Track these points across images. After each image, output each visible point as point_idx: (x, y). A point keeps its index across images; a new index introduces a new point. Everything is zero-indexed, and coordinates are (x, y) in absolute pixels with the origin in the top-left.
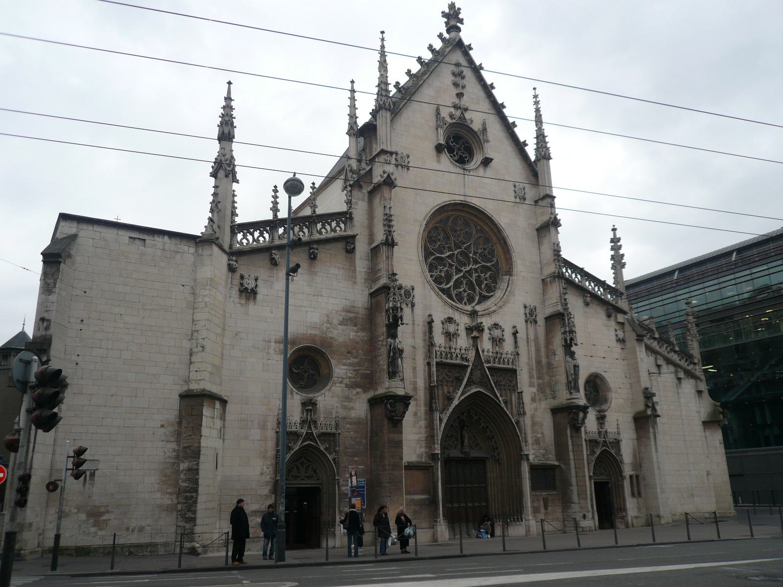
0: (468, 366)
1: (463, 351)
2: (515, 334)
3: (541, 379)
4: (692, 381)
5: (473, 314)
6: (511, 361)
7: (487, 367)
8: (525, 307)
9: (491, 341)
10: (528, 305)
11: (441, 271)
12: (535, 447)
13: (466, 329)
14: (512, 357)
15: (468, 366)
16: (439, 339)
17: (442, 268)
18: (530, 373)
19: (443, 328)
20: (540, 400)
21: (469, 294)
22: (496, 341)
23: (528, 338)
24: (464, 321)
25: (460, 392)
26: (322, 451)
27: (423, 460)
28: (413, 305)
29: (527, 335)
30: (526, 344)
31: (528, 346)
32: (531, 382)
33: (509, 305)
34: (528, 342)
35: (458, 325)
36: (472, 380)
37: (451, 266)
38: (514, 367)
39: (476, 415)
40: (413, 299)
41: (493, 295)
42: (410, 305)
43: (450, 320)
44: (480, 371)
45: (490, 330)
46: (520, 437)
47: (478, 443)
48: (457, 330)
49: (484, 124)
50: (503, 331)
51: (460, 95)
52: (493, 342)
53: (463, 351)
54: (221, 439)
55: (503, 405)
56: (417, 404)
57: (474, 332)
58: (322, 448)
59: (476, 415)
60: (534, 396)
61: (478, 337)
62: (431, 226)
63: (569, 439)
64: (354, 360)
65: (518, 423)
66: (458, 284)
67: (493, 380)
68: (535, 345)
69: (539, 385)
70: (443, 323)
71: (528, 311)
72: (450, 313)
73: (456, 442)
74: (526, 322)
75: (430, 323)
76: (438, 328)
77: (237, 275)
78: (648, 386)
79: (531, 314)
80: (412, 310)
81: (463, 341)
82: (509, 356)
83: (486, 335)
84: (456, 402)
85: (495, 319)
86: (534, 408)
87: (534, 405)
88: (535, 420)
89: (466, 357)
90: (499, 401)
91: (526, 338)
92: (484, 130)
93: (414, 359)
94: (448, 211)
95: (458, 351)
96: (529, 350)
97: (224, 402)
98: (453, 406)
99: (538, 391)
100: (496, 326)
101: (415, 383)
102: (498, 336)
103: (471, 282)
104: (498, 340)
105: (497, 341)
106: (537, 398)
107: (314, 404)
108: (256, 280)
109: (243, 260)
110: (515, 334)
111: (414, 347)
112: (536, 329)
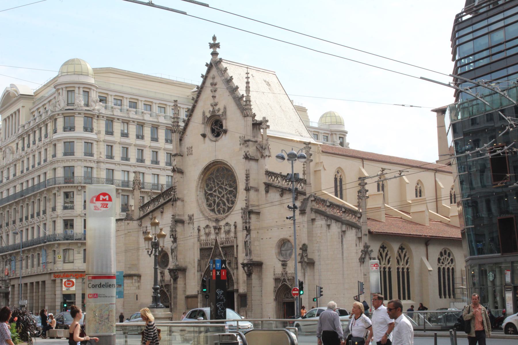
2: (236, 227)
4: (354, 231)
5: (217, 221)
7: (222, 247)
16: (203, 238)
24: (212, 224)
26: (165, 292)
28: (193, 224)
37: (215, 196)
43: (207, 226)
49: (225, 108)
51: (214, 97)
54: (139, 289)
57: (218, 229)
58: (165, 291)
61: (218, 233)
62: (205, 178)
72: (207, 223)
75: (199, 230)
76: (202, 232)
77: (142, 227)
78: (306, 242)
80: (193, 225)
81: (213, 237)
83: (222, 230)
85: (227, 220)
92: (225, 112)
94: (211, 168)
95: (202, 242)
97: (139, 276)
100: (227, 224)
101: (194, 260)
105: (228, 232)
107: (164, 274)
108: (147, 227)
109: (143, 220)
110: (236, 227)
111: (194, 243)
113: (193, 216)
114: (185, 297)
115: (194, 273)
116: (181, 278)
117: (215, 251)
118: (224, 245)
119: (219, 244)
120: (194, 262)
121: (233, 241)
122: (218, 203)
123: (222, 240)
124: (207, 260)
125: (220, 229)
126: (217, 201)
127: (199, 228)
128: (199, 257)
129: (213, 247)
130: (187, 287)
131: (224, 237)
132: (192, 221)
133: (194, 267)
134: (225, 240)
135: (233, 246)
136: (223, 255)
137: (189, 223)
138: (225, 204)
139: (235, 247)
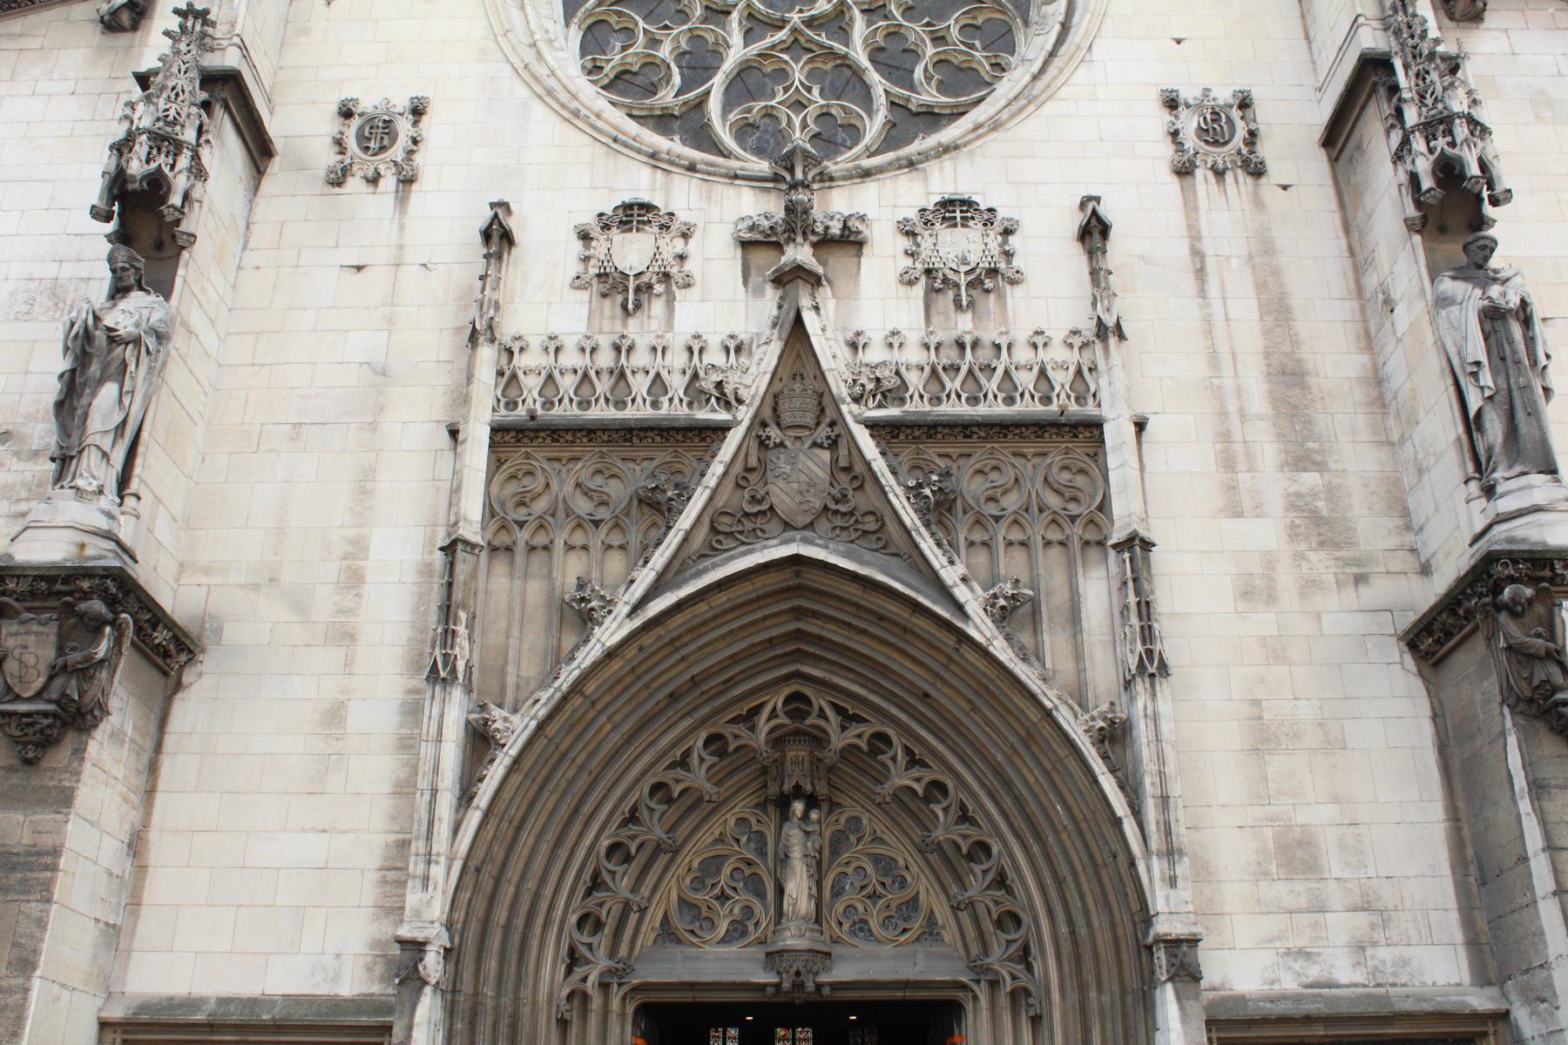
0: (722, 430)
1: (715, 357)
3: (1321, 467)
6: (1061, 379)
7: (873, 426)
8: (1172, 104)
9: (919, 290)
10: (1188, 94)
11: (799, 105)
12: (1281, 891)
13: (745, 245)
14: (1073, 357)
15: (722, 430)
17: (786, 90)
18: (1225, 437)
19: (586, 259)
20: (1309, 586)
21: (824, 115)
22: (957, 286)
23: (1197, 254)
25: (645, 577)
27: (810, 1035)
29: (1194, 236)
30: (1188, 282)
31: (1202, 293)
32: (1232, 488)
33: (1047, 109)
34: (1200, 273)
35: (685, 236)
36: (764, 507)
38: (1090, 409)
39: (848, 718)
40: (410, 153)
41: (980, 100)
42: (389, 182)
43: (633, 215)
44: (826, 455)
45: (911, 234)
46: (1130, 827)
47: (913, 903)
48: (682, 258)
50: (1007, 232)
52: (931, 292)
53: (715, 357)
55: (981, 627)
56: (348, 663)
59: (848, 718)
60: (1256, 569)
63: (1525, 806)
64: (22, 466)
65: (1114, 736)
66: (745, 83)
67: (914, 492)
68: (1261, 287)
69: (1295, 503)
70: (585, 237)
71: (1189, 124)
73: (743, 898)
74: (1184, 171)
79: (1214, 130)
82: (1056, 354)
84: (611, 631)
85: (943, 180)
86: (1263, 641)
87: (1264, 622)
88: (1267, 716)
89: (719, 385)
90: (959, 608)
91: (1186, 252)
93: (373, 427)
96: (1208, 321)
98: (589, 655)
99: (1293, 534)
101: (358, 547)
102: (965, 262)
103: (845, 63)
104: (963, 281)
106: (1286, 581)
112: (1258, 203)
113: (417, 112)
114: (104, 1025)
115: (335, 715)
116: (117, 736)
117: (746, 474)
118: (916, 407)
119: (839, 388)
120: (354, 579)
121: (1061, 379)
122: (745, 69)
123: (875, 354)
124: (615, 563)
125: (849, 240)
126: (737, 51)
127: (512, 224)
128: (473, 507)
129: (745, 414)
130: (161, 885)
131: (914, 336)
132: (397, 152)
133: (345, 636)
134: (913, 355)
135: (1094, 427)
136: (910, 517)
137: (338, 179)
138: (846, 79)
139: (1117, 433)
